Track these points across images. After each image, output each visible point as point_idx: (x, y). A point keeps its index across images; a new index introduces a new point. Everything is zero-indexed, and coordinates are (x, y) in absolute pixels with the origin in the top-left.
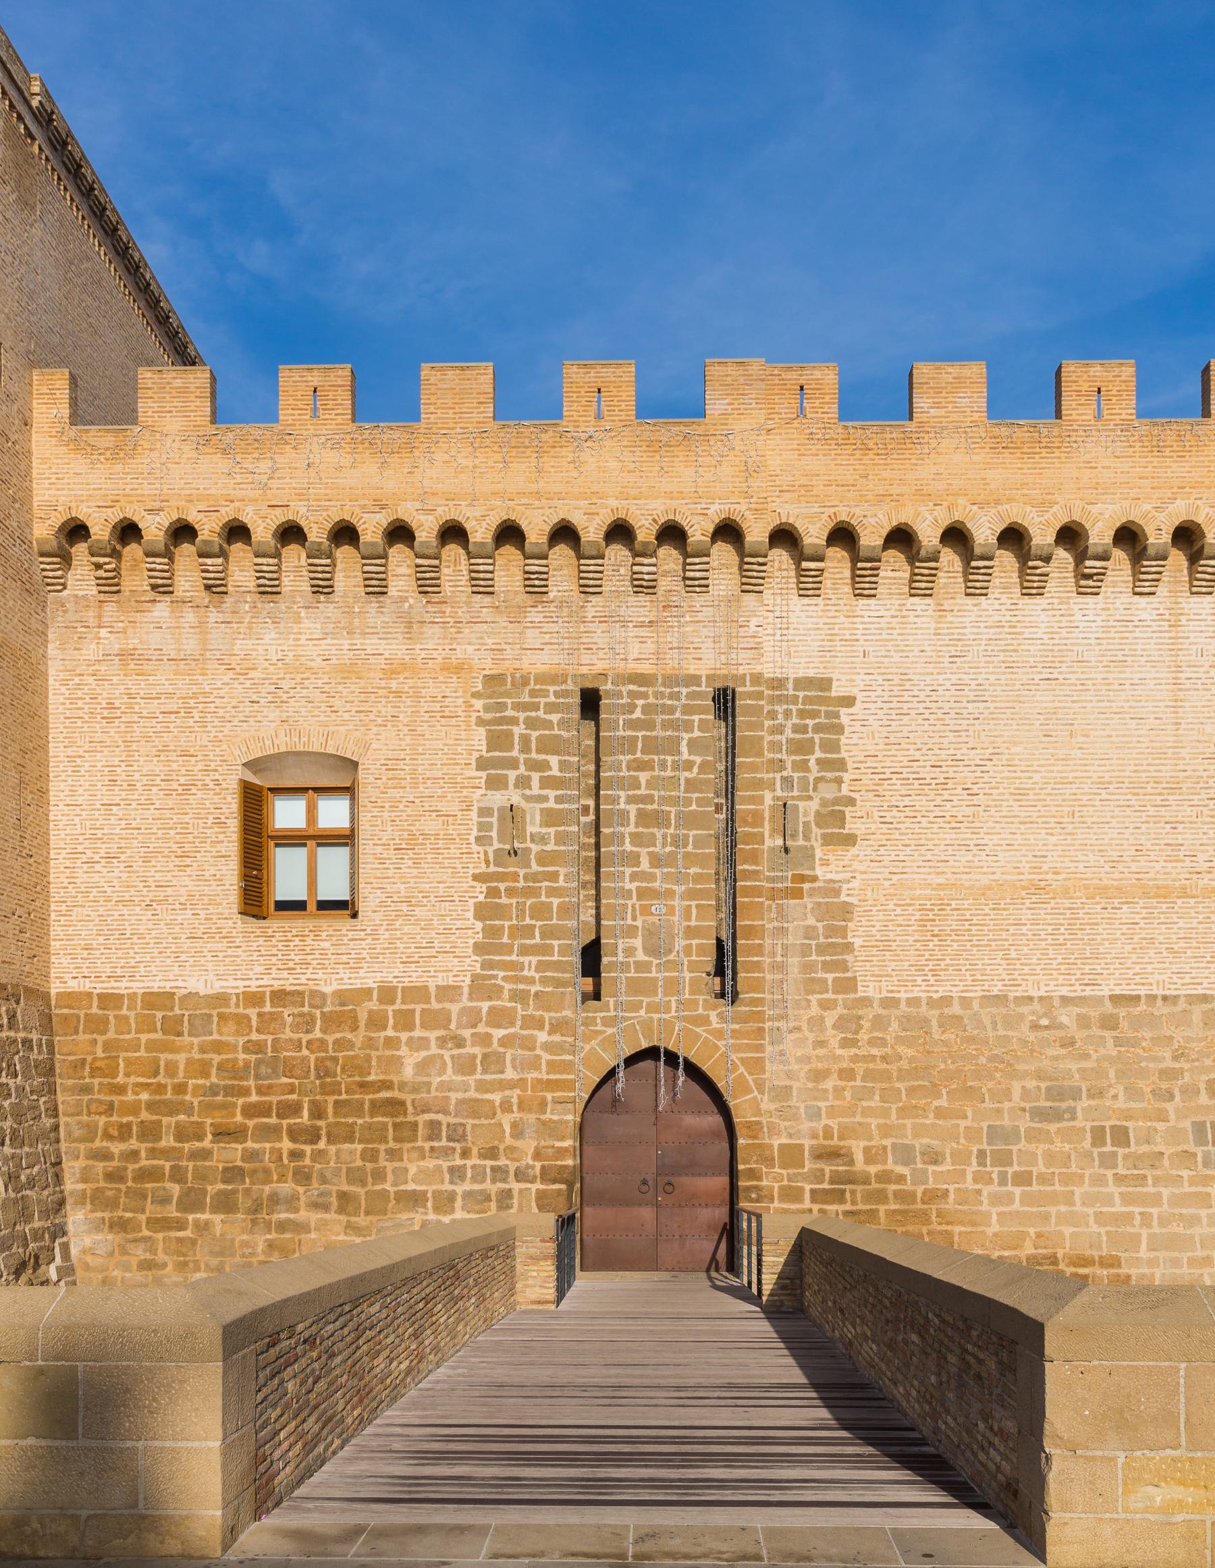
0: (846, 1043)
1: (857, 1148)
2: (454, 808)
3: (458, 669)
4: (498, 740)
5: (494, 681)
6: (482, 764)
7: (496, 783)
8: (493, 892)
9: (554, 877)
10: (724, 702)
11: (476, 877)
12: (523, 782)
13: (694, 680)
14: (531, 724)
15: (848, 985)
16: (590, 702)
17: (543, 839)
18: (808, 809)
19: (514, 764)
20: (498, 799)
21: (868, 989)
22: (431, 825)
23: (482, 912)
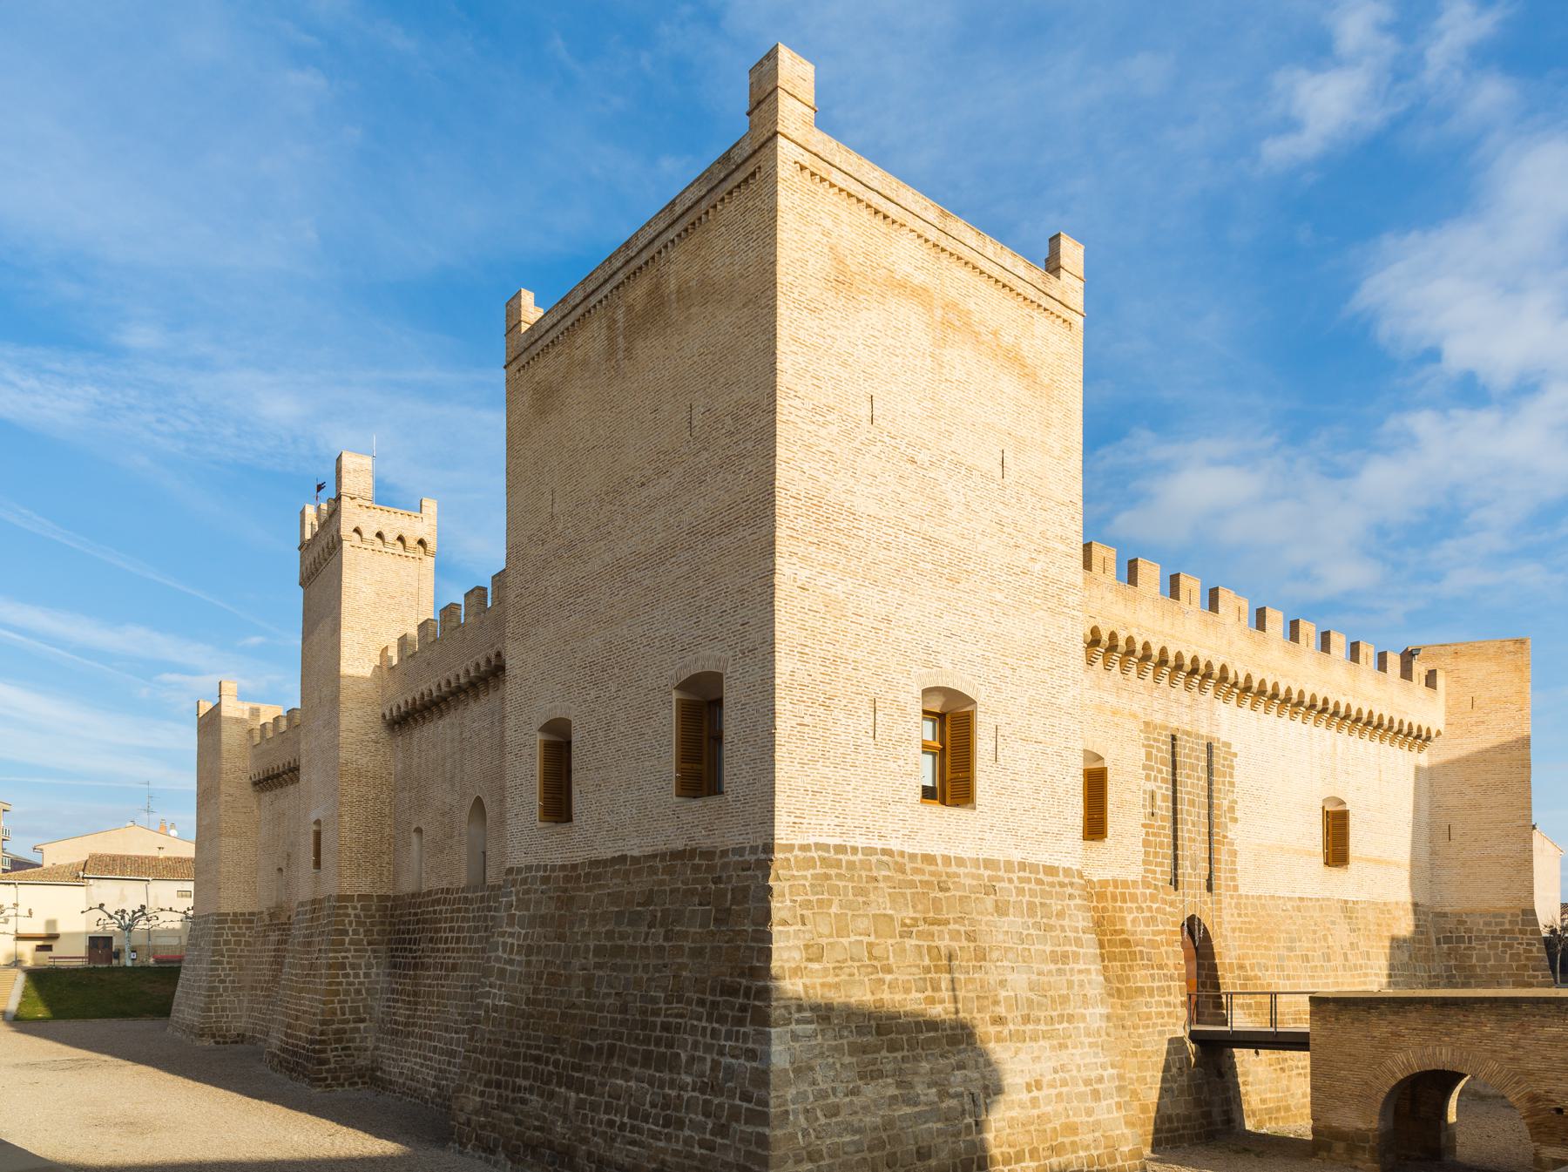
0: (1239, 915)
1: (1247, 963)
2: (1134, 788)
3: (1134, 716)
4: (1149, 756)
5: (1147, 724)
6: (1145, 767)
7: (1148, 778)
8: (1147, 834)
9: (1163, 828)
10: (1210, 747)
11: (1144, 826)
12: (1156, 779)
13: (1199, 736)
14: (1159, 750)
15: (1236, 888)
16: (1174, 738)
17: (1161, 808)
18: (1226, 803)
19: (1152, 768)
20: (1150, 786)
21: (1242, 891)
22: (1128, 796)
23: (1146, 843)
